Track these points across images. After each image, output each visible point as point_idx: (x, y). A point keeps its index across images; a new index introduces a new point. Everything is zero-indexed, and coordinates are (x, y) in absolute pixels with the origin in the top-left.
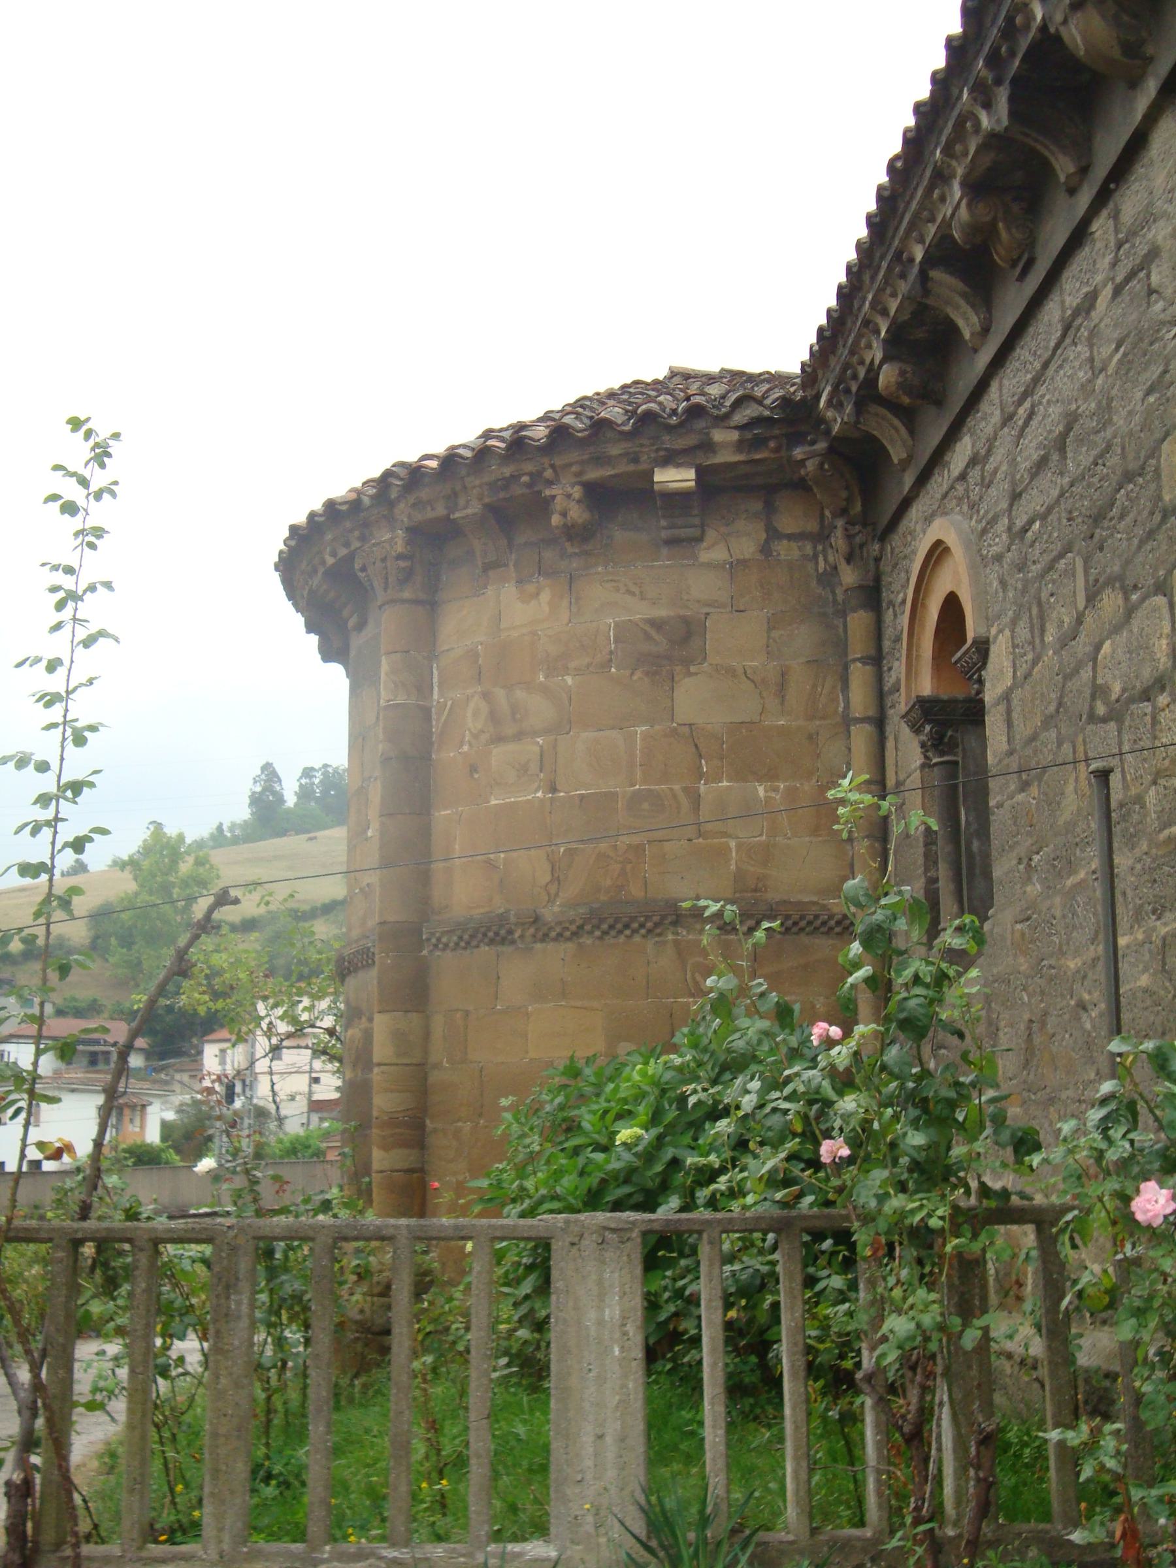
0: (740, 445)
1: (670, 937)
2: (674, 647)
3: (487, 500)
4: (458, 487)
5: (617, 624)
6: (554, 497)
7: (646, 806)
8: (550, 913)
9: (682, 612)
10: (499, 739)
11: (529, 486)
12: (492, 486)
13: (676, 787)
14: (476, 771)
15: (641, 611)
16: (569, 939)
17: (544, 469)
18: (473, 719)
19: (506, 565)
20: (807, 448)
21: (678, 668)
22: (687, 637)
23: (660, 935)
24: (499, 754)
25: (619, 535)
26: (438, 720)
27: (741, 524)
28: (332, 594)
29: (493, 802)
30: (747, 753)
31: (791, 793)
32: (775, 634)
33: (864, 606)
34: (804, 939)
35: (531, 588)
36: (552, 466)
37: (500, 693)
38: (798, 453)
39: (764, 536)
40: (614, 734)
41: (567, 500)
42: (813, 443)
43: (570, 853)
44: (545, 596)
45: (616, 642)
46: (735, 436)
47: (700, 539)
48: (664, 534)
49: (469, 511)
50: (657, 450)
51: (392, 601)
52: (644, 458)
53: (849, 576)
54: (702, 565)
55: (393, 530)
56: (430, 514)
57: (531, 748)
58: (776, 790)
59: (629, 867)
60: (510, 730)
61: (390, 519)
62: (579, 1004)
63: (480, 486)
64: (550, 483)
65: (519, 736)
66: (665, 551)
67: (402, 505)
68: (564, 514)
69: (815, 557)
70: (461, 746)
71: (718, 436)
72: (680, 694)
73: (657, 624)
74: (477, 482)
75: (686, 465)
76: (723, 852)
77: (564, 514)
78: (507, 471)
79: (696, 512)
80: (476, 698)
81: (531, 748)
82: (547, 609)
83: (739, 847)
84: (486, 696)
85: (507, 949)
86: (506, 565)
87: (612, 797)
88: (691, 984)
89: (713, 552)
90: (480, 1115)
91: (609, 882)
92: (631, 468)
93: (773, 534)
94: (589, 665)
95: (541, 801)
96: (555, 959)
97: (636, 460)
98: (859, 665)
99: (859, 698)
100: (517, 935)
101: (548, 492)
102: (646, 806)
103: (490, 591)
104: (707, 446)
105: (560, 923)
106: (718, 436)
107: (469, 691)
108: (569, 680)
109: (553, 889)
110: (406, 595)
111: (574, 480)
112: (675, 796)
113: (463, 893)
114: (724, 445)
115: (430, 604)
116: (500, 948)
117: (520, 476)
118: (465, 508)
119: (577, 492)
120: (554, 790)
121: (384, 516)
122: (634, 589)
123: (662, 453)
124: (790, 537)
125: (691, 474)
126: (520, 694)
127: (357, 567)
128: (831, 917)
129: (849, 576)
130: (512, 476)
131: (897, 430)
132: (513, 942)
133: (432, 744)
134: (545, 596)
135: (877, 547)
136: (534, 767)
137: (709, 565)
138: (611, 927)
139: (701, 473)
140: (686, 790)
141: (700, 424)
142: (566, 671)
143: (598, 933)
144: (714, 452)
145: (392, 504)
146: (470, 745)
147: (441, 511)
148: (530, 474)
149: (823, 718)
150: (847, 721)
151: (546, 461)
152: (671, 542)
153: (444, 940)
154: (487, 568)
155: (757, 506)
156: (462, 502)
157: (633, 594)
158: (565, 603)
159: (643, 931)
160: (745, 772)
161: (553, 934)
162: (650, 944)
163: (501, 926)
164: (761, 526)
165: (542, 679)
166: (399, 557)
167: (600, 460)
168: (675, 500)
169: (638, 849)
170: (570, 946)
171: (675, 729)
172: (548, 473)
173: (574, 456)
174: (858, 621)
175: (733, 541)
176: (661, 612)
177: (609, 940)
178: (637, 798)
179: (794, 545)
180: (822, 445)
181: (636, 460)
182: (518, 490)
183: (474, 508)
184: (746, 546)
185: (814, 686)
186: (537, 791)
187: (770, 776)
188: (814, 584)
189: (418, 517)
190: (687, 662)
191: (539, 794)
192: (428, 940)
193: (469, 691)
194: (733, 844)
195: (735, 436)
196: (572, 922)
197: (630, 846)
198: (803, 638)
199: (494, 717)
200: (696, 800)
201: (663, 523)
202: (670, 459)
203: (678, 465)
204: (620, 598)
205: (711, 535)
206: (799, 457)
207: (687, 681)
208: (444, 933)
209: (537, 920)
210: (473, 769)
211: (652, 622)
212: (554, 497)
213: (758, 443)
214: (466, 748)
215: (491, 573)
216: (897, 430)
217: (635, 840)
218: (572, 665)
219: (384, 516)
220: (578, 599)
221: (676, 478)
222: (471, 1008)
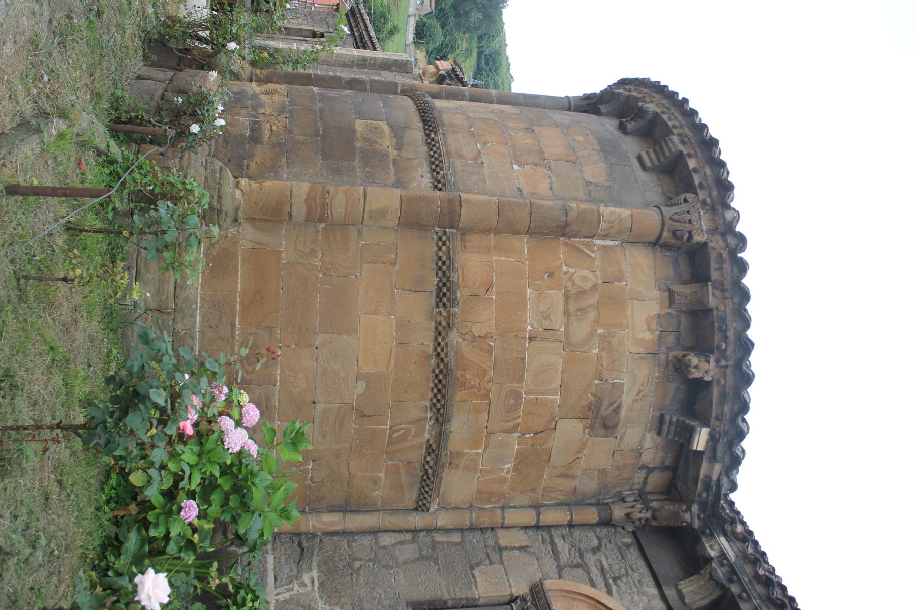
0: (708, 478)
1: (429, 415)
2: (602, 418)
3: (715, 313)
4: (728, 295)
5: (622, 384)
6: (708, 362)
7: (512, 401)
8: (454, 337)
9: (621, 424)
10: (567, 298)
11: (719, 347)
12: (723, 320)
13: (519, 420)
14: (549, 276)
15: (626, 400)
16: (435, 349)
17: (727, 361)
18: (584, 275)
19: (670, 307)
20: (697, 513)
21: (589, 422)
22: (606, 427)
23: (431, 409)
24: (557, 296)
25: (673, 386)
26: (582, 243)
27: (661, 454)
28: (667, 153)
29: (529, 291)
30: (532, 459)
31: (505, 480)
32: (596, 473)
33: (600, 520)
34: (417, 486)
35: (654, 325)
36: (727, 367)
37: (593, 300)
38: (695, 508)
39: (650, 466)
40: (558, 382)
41: (703, 368)
42: (699, 518)
43: (490, 350)
44: (648, 336)
45: (613, 384)
46: (715, 477)
47: (659, 433)
48: (667, 418)
49: (711, 298)
50: (720, 433)
51: (663, 224)
52: (717, 423)
53: (618, 513)
54: (644, 434)
55: (708, 232)
56: (713, 265)
57: (558, 322)
58: (508, 473)
59: (476, 390)
60: (572, 307)
61: (713, 231)
62: (393, 355)
63: (725, 311)
64: (718, 362)
65: (567, 313)
66: (657, 414)
67: (722, 243)
68: (696, 367)
69: (632, 490)
70: (566, 265)
71: (718, 467)
72: (575, 422)
73: (617, 411)
74: (728, 310)
75: (706, 449)
76: (476, 445)
77: (696, 367)
78: (730, 334)
79: (676, 439)
80: (594, 279)
81: (558, 322)
82: (640, 336)
83: (478, 454)
84: (595, 287)
85: (433, 299)
86: (670, 307)
87: (521, 380)
88: (398, 427)
89: (650, 440)
90: (325, 274)
91: (468, 377)
92: (714, 415)
93: (650, 470)
94: (602, 365)
95: (524, 330)
96: (424, 340)
97: (717, 418)
98: (569, 518)
99: (551, 517)
100: (442, 309)
101: (712, 360)
102: (512, 401)
103: (656, 293)
104: (713, 458)
105: (447, 346)
106: (718, 467)
107: (598, 274)
108: (595, 351)
109: (468, 337)
110: (665, 234)
111: (716, 378)
112: (514, 419)
113: (473, 264)
114: (712, 468)
115: (656, 244)
116: (434, 294)
117: (726, 343)
118: (713, 294)
119: (707, 378)
120: (531, 339)
121: (717, 228)
122: (641, 395)
123: (717, 436)
124: (646, 478)
125: (700, 448)
126: (593, 314)
127: (688, 195)
128: (429, 502)
129: (618, 513)
130: (727, 337)
131: (702, 599)
132: (437, 306)
133: (570, 238)
134: (648, 336)
135: (631, 529)
136: (547, 324)
137: (643, 438)
138: (440, 381)
139: (699, 454)
140: (518, 425)
141: (727, 459)
142: (602, 349)
143: (437, 371)
144: (710, 462)
145: (723, 235)
146: (566, 273)
147: (714, 275)
148: (725, 350)
149: (543, 495)
150: (537, 507)
151: (731, 363)
152: (661, 419)
153: (444, 248)
154: (671, 293)
155: (668, 463)
156: (717, 293)
157: (638, 395)
158: (641, 350)
159: (435, 400)
160: (522, 460)
161: (440, 339)
162: (427, 403)
163: (449, 300)
164: (657, 464)
165: (599, 331)
166: (690, 237)
167: (723, 397)
168: (689, 434)
169: (486, 396)
170: (430, 350)
171: (554, 419)
172: (723, 363)
173: (730, 381)
174: (592, 515)
175: (650, 448)
176: (623, 412)
177: (432, 376)
178: (517, 395)
179: (642, 480)
180: (697, 524)
181: (717, 418)
182: (717, 339)
183: (712, 302)
184: (647, 458)
185: (562, 491)
186: (532, 326)
187: (516, 469)
188: (617, 489)
189: (713, 255)
190: (591, 427)
191: (529, 328)
192: (445, 233)
193: (598, 274)
194: (480, 451)
195: (715, 477)
196: (447, 356)
197: (488, 391)
198: (589, 485)
199: (582, 293)
200: (510, 431)
201: (675, 419)
202: (712, 438)
203: (707, 442)
204: (638, 386)
205: (659, 440)
206: (693, 509)
207: (581, 427)
208: (448, 248)
209: (449, 327)
210: (551, 275)
211: (619, 407)
212: (708, 362)
213: (707, 486)
214: (564, 269)
215: (667, 294)
216: (702, 599)
217: (492, 395)
218: (604, 354)
219: (717, 228)
220: (642, 358)
221: (701, 440)
222: (397, 268)
